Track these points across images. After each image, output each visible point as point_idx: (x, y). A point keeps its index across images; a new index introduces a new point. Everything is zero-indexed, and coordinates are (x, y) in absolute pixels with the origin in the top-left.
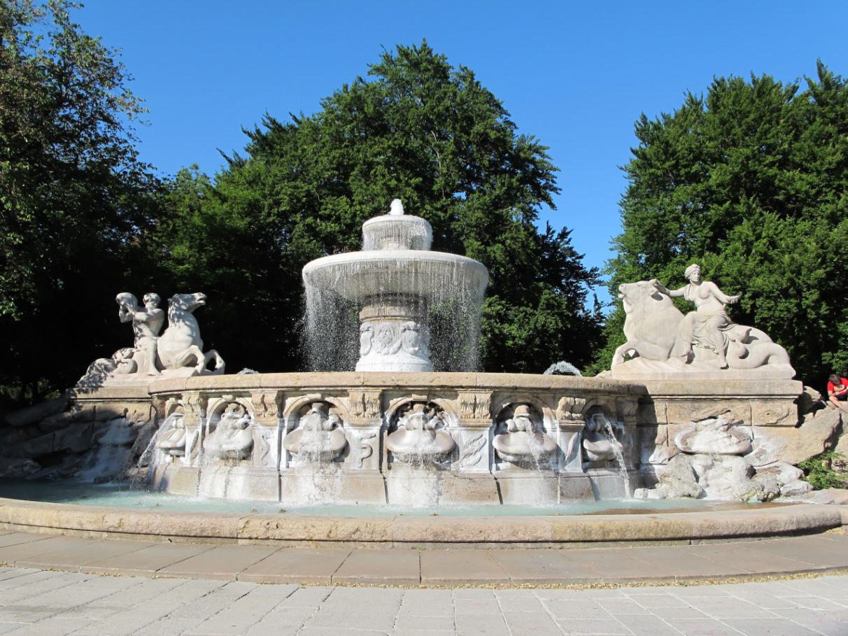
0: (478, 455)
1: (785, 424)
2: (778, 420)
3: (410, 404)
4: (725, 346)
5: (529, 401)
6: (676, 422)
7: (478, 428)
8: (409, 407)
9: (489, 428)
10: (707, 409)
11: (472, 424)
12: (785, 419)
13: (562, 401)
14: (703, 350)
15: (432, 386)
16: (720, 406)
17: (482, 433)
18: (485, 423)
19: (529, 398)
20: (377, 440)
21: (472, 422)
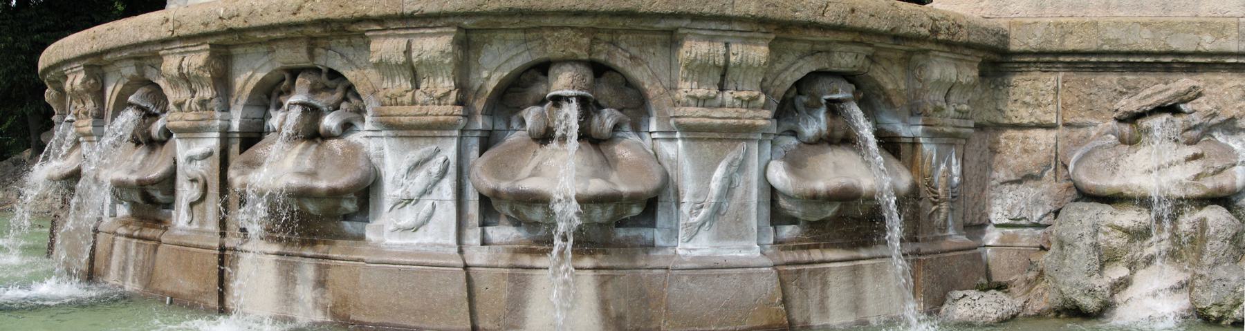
0: (427, 204)
3: (287, 76)
5: (584, 55)
6: (1080, 120)
7: (427, 133)
8: (285, 83)
9: (456, 133)
10: (1157, 89)
11: (405, 120)
13: (695, 49)
15: (297, 25)
16: (1183, 82)
17: (439, 143)
18: (441, 118)
19: (576, 45)
20: (215, 162)
21: (407, 114)
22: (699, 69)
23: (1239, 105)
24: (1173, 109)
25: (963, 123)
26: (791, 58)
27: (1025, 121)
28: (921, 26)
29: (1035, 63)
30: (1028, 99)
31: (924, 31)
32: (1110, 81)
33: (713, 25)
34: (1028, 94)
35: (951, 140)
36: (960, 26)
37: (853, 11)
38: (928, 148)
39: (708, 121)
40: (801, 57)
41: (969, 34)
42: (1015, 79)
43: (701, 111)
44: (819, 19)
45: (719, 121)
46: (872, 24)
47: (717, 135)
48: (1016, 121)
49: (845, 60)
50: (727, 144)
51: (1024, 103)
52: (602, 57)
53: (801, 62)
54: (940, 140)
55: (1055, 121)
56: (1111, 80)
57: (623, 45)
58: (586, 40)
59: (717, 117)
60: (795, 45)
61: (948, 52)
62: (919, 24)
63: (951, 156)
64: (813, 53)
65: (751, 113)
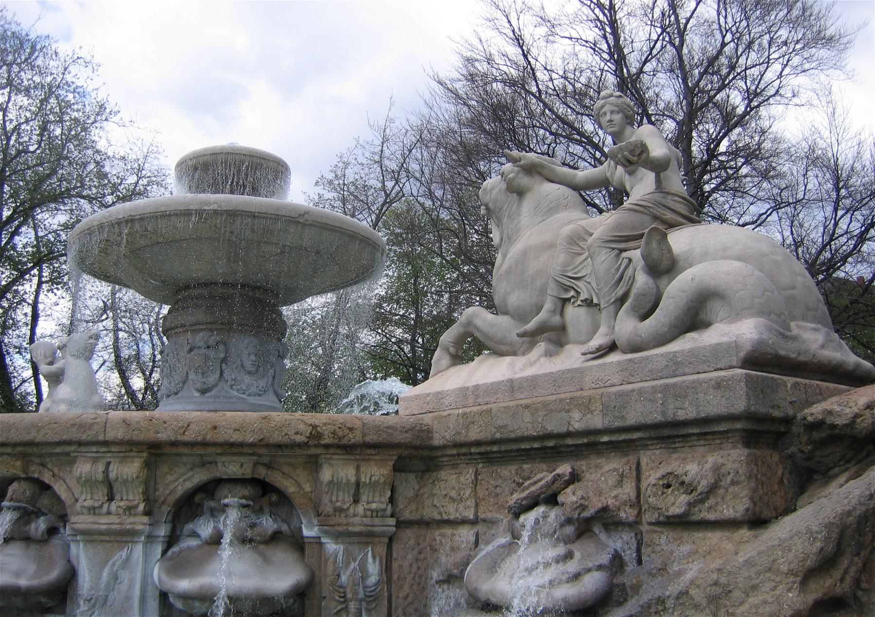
1: (711, 516)
2: (690, 505)
4: (620, 291)
12: (711, 501)
13: (83, 468)
14: (582, 312)
19: (14, 466)
22: (89, 483)
23: (615, 493)
24: (552, 500)
25: (377, 521)
26: (182, 470)
27: (452, 517)
28: (297, 433)
29: (459, 455)
30: (453, 494)
31: (299, 439)
32: (510, 472)
33: (94, 449)
34: (454, 488)
35: (364, 539)
36: (351, 429)
37: (215, 428)
38: (331, 546)
39: (96, 526)
40: (192, 469)
41: (364, 435)
42: (443, 474)
43: (90, 518)
44: (180, 438)
45: (105, 527)
46: (236, 437)
47: (107, 538)
48: (445, 517)
49: (232, 468)
50: (116, 545)
51: (451, 498)
52: (36, 475)
53: (190, 474)
54: (349, 540)
55: (472, 517)
56: (508, 471)
57: (50, 466)
58: (18, 463)
59: (103, 523)
60: (185, 459)
61: (341, 454)
62: (293, 432)
63: (367, 554)
64: (203, 465)
65: (132, 519)
